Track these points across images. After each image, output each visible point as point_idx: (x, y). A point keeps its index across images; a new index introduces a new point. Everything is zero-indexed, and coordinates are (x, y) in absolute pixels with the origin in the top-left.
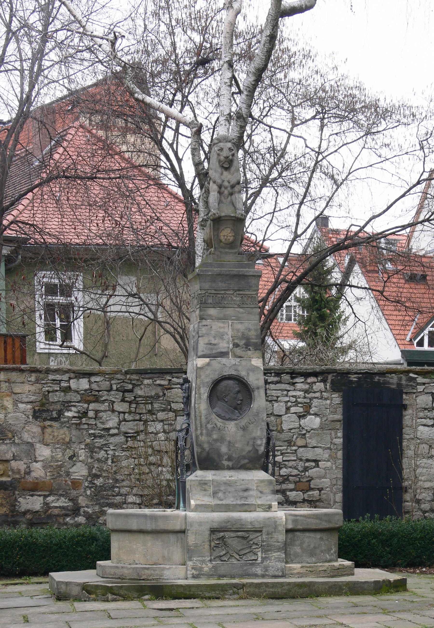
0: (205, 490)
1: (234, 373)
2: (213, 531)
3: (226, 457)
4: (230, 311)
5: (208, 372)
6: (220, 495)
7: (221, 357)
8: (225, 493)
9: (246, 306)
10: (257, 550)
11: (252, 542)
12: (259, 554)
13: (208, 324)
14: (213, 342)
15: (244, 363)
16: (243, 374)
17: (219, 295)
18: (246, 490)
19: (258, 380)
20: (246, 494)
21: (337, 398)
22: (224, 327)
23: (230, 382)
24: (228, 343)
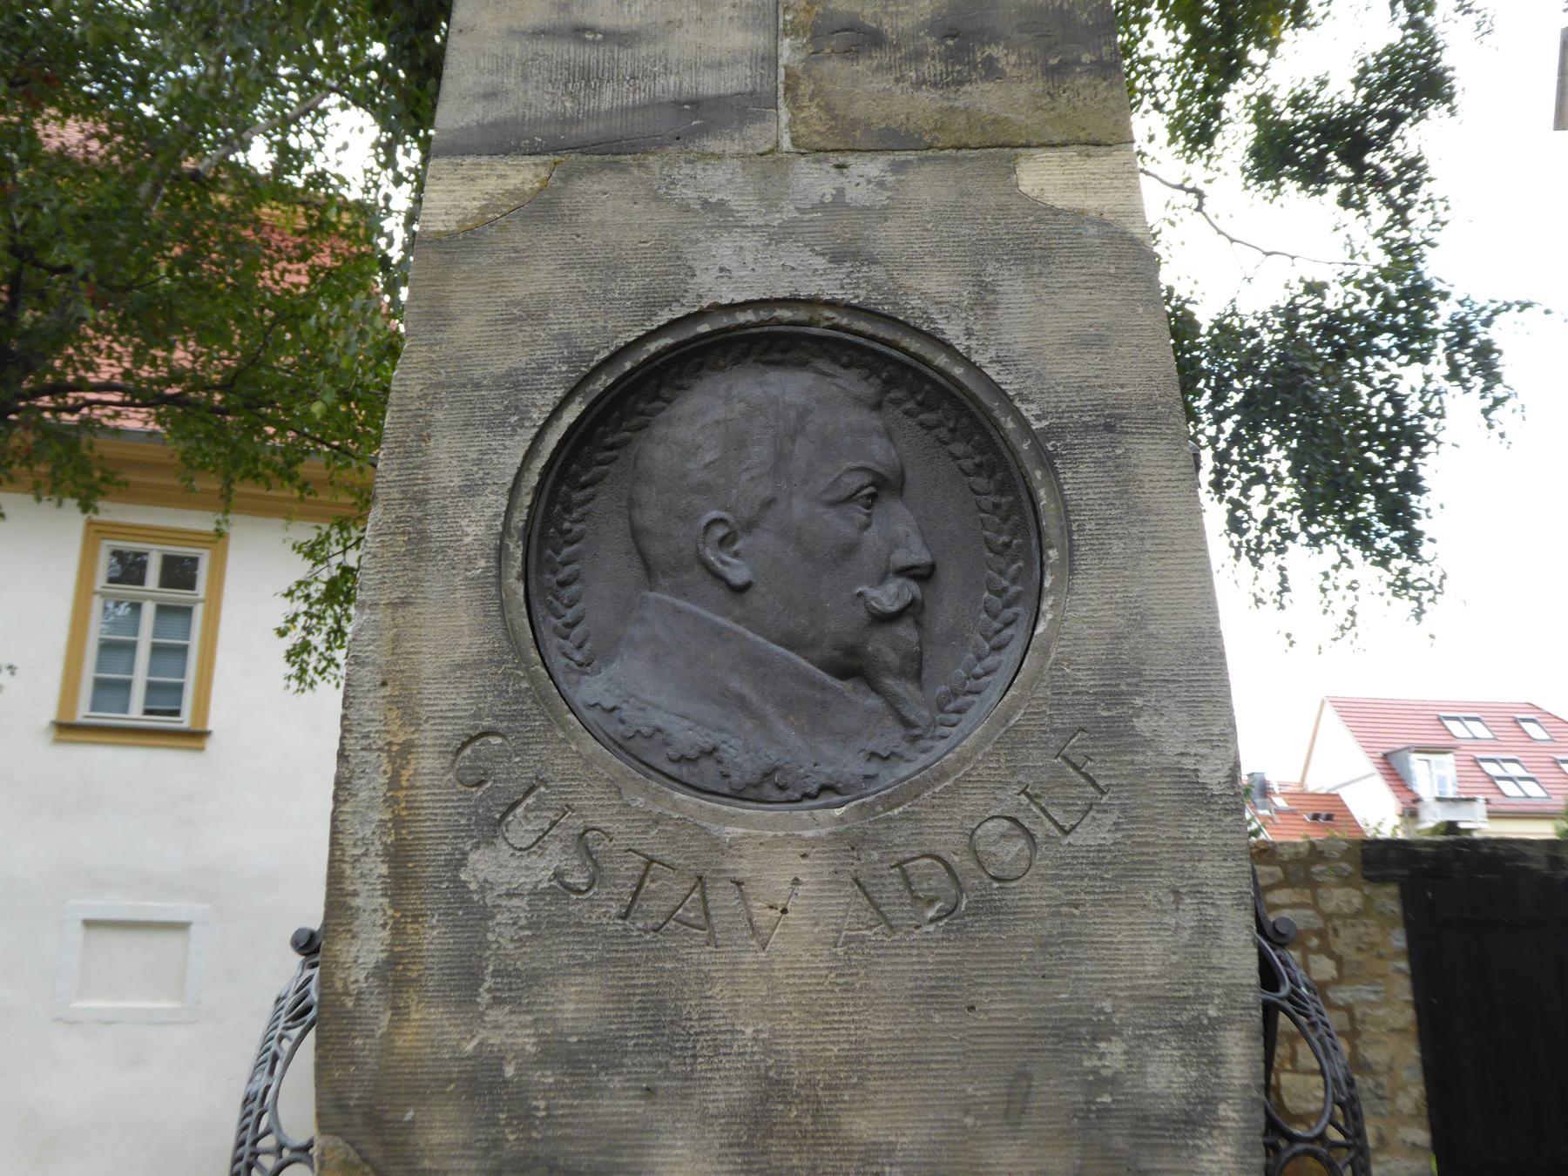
1: (819, 278)
5: (541, 277)
15: (929, 186)
16: (930, 290)
21: (1388, 899)
23: (790, 386)
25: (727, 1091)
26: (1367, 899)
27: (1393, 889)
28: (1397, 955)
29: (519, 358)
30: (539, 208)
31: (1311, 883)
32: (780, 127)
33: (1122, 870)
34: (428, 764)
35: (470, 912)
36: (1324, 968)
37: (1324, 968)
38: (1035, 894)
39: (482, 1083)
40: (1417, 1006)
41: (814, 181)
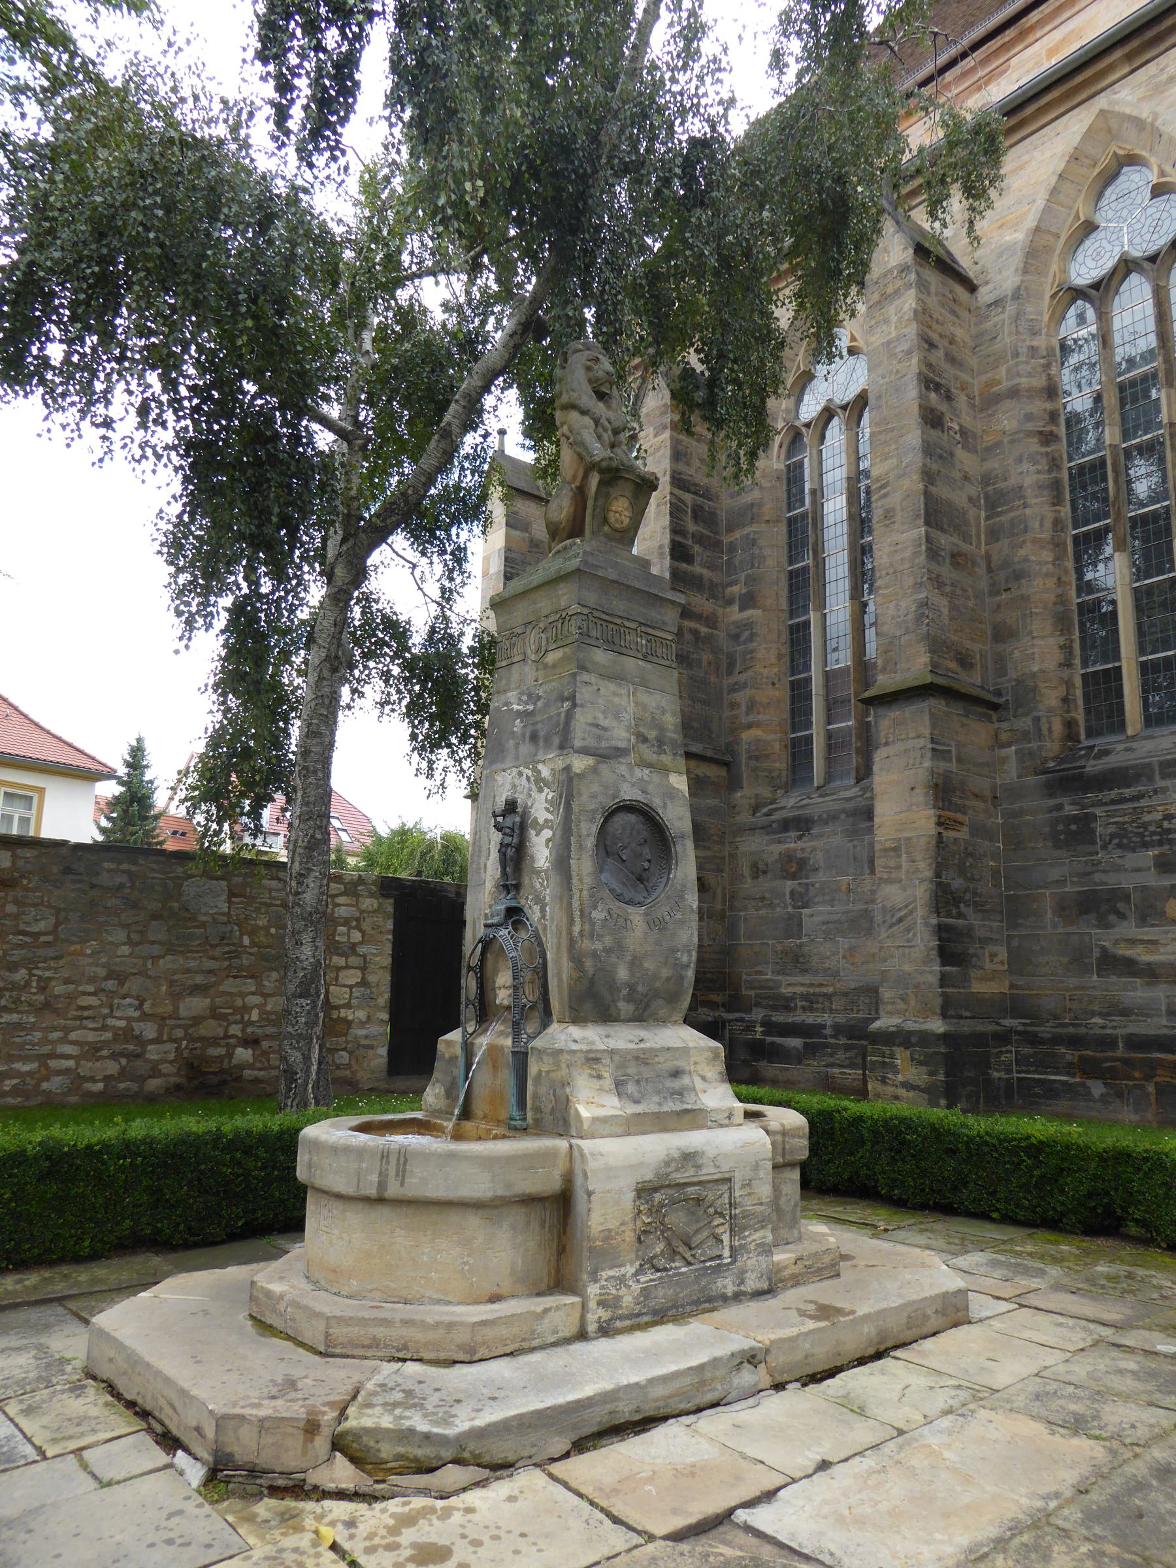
0: (599, 1077)
2: (644, 1191)
3: (625, 992)
4: (631, 664)
5: (595, 788)
6: (631, 1088)
7: (617, 757)
8: (638, 1082)
9: (655, 659)
10: (720, 1230)
11: (711, 1210)
12: (726, 1238)
13: (593, 680)
14: (605, 723)
15: (656, 778)
16: (657, 802)
17: (611, 626)
18: (676, 1074)
19: (680, 819)
20: (676, 1084)
21: (389, 905)
22: (620, 695)
23: (633, 818)
24: (628, 728)
25: (628, 958)
26: (380, 904)
27: (392, 901)
28: (388, 932)
29: (593, 806)
30: (594, 770)
31: (357, 895)
32: (632, 758)
33: (682, 922)
34: (585, 893)
35: (592, 923)
36: (356, 936)
37: (356, 936)
38: (670, 926)
39: (594, 954)
40: (393, 956)
41: (638, 773)
